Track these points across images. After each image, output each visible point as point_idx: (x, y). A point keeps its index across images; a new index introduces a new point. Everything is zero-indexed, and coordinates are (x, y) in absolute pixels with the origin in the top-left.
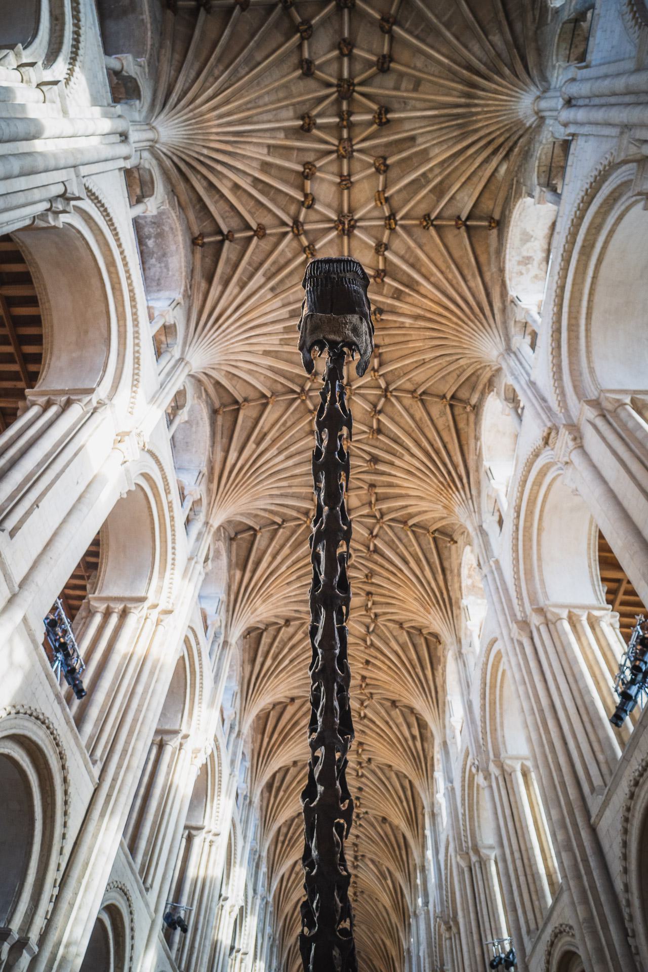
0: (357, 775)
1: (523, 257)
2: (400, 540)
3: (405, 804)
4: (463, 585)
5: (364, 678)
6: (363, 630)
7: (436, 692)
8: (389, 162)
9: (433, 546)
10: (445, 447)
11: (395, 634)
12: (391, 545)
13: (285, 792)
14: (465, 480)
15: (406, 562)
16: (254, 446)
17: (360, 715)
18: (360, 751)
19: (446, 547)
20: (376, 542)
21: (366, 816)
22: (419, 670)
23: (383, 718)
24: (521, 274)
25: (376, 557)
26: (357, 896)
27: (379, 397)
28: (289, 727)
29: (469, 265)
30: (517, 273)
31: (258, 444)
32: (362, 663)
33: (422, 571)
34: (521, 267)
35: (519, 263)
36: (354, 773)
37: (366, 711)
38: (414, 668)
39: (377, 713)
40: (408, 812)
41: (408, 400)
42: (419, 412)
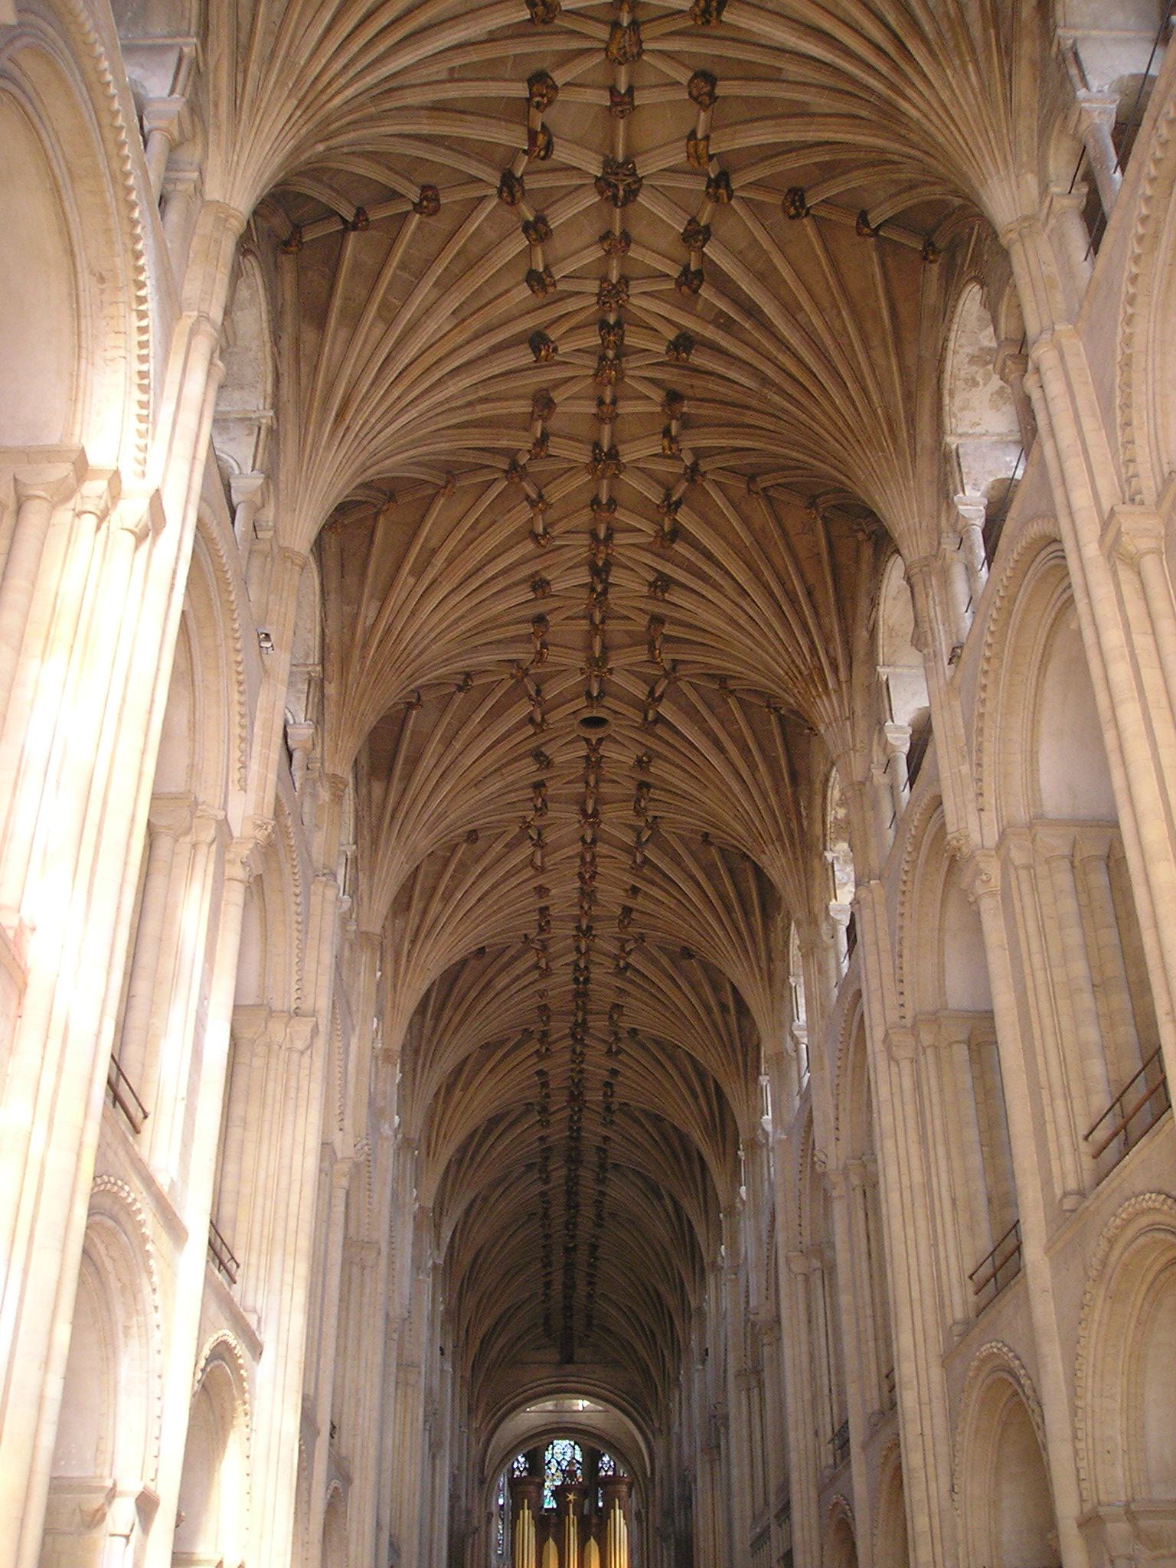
0: (610, 1050)
1: (981, 349)
2: (710, 708)
3: (702, 1101)
4: (830, 818)
5: (627, 911)
6: (629, 839)
7: (770, 959)
8: (719, 91)
9: (776, 731)
10: (809, 594)
11: (694, 847)
12: (691, 713)
13: (465, 1089)
14: (843, 676)
15: (722, 750)
16: (412, 581)
17: (618, 965)
18: (615, 1017)
19: (801, 734)
20: (660, 710)
21: (626, 1108)
22: (738, 914)
23: (663, 970)
24: (975, 384)
25: (659, 730)
26: (603, 1219)
27: (679, 478)
28: (473, 994)
29: (876, 315)
30: (966, 381)
31: (418, 573)
32: (626, 891)
33: (752, 767)
34: (975, 368)
35: (973, 360)
36: (604, 1048)
37: (630, 960)
38: (729, 910)
39: (654, 961)
40: (705, 1109)
41: (739, 486)
42: (761, 514)
